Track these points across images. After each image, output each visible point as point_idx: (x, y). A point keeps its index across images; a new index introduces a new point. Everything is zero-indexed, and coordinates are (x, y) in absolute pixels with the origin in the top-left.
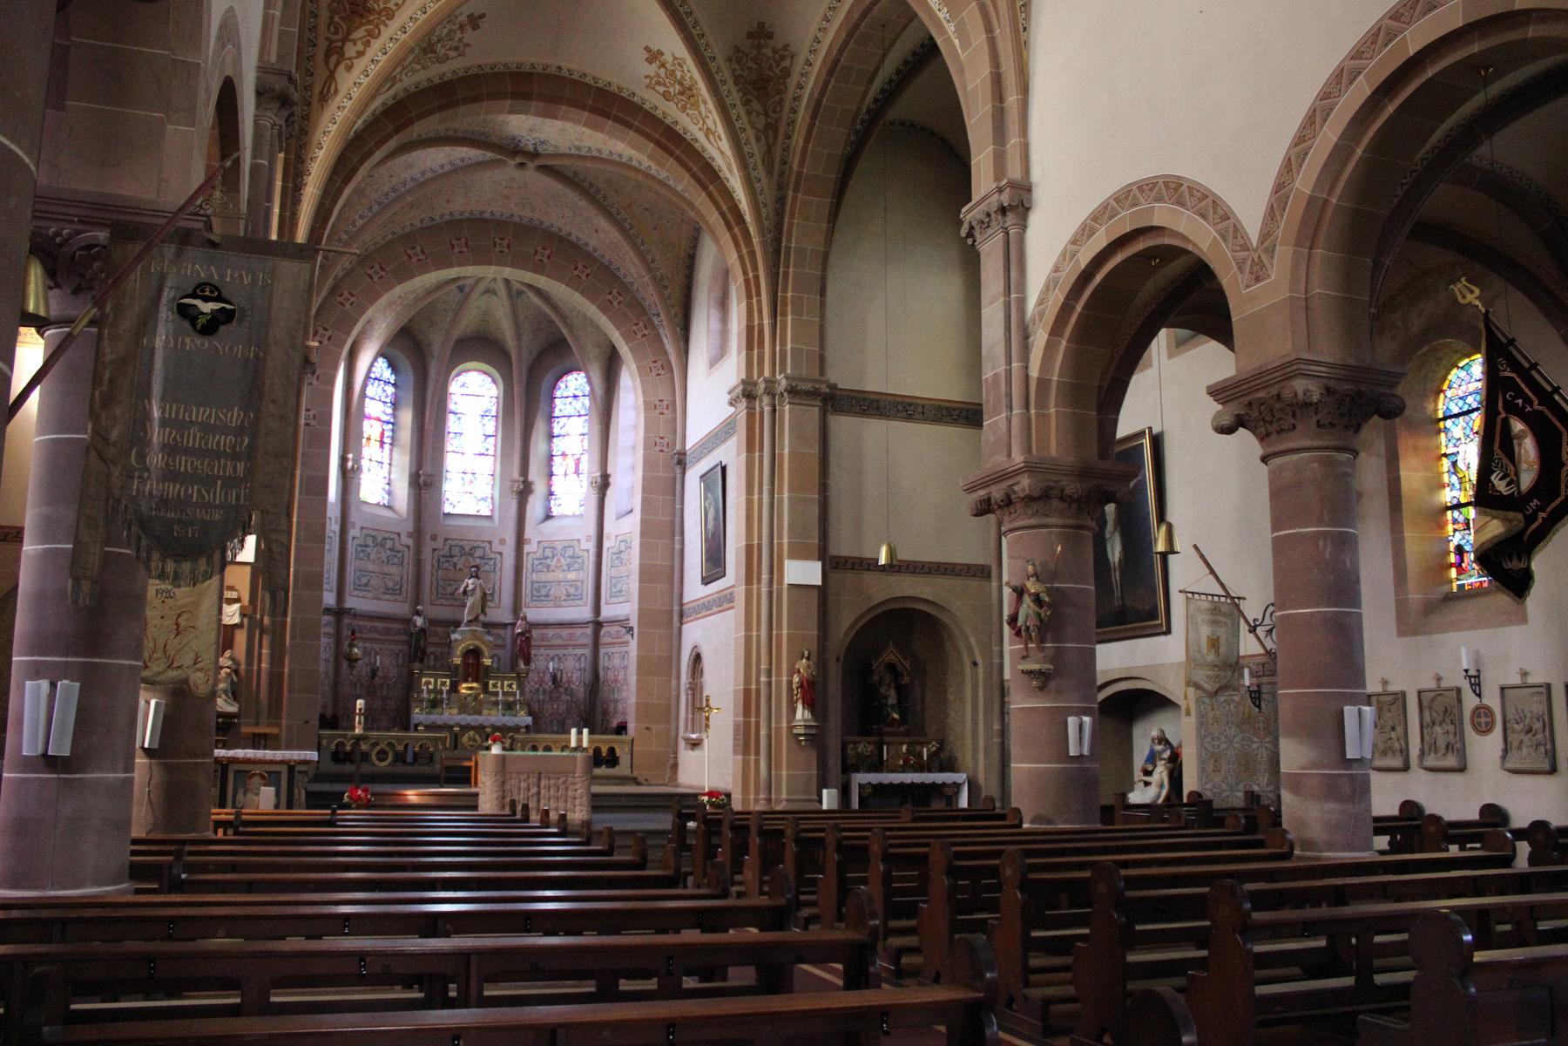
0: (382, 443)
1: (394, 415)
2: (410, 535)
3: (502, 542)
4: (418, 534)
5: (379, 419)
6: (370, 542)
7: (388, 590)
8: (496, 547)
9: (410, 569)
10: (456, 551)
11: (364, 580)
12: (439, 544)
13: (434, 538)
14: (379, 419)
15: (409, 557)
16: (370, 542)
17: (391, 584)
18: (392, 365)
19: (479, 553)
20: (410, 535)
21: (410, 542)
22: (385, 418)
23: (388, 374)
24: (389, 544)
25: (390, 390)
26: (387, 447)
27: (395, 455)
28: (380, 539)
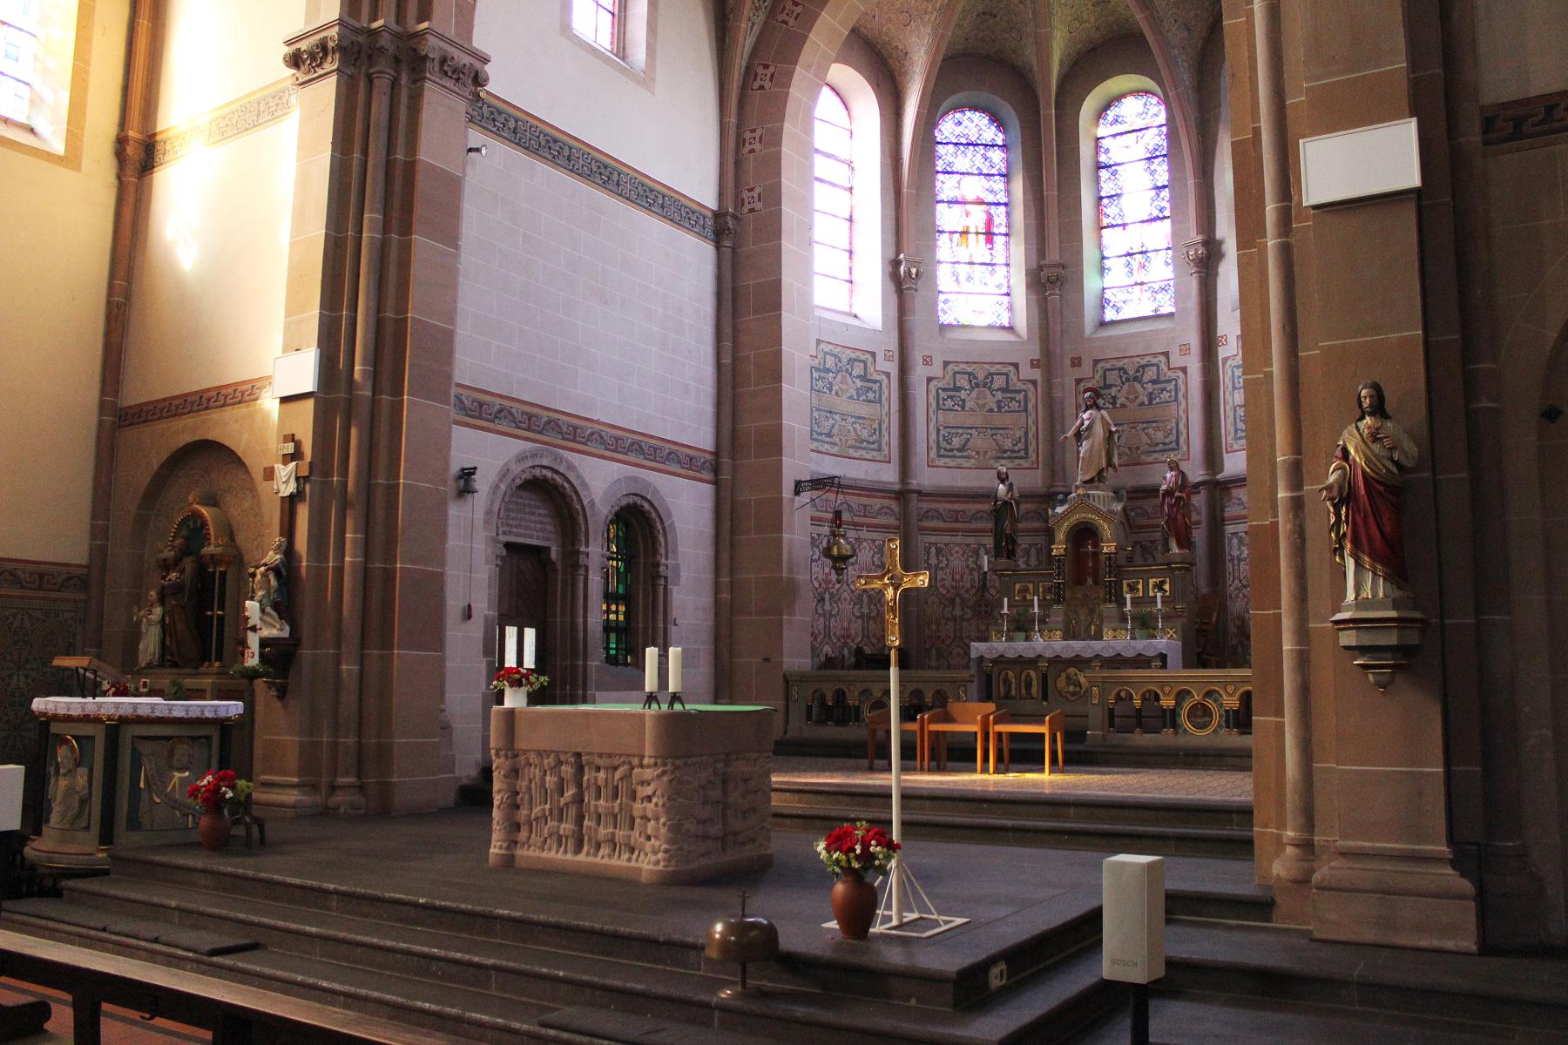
0: (989, 235)
1: (1008, 192)
2: (1034, 364)
3: (1184, 350)
4: (1046, 362)
5: (980, 202)
6: (963, 382)
7: (1002, 453)
8: (1176, 360)
9: (1036, 419)
10: (1113, 378)
11: (956, 442)
12: (1086, 370)
13: (1077, 362)
14: (980, 202)
15: (1035, 397)
16: (963, 382)
17: (1008, 444)
18: (996, 119)
19: (1151, 374)
20: (1034, 364)
21: (1036, 374)
22: (990, 198)
23: (991, 133)
24: (999, 382)
25: (997, 156)
26: (999, 241)
27: (1012, 247)
28: (978, 377)
